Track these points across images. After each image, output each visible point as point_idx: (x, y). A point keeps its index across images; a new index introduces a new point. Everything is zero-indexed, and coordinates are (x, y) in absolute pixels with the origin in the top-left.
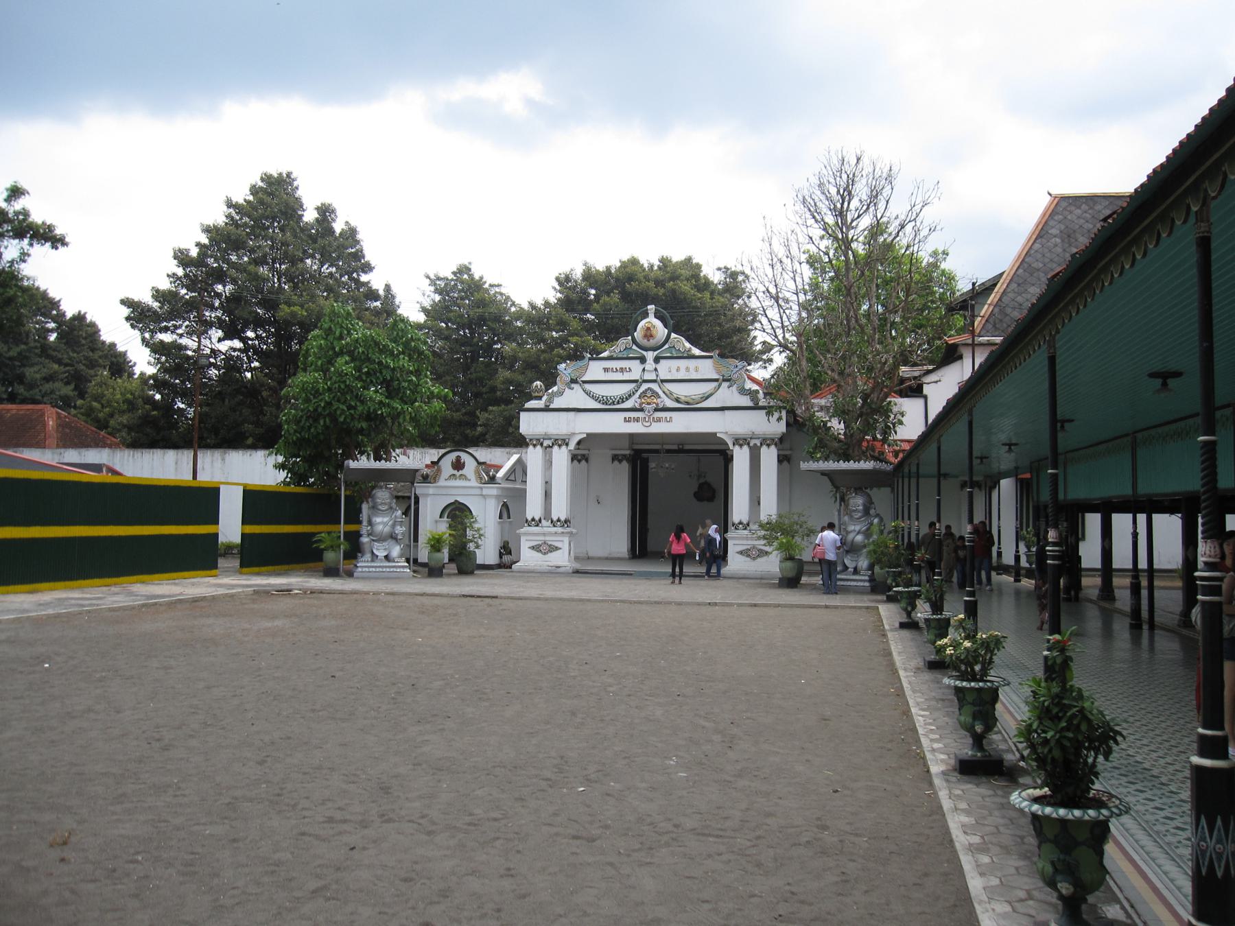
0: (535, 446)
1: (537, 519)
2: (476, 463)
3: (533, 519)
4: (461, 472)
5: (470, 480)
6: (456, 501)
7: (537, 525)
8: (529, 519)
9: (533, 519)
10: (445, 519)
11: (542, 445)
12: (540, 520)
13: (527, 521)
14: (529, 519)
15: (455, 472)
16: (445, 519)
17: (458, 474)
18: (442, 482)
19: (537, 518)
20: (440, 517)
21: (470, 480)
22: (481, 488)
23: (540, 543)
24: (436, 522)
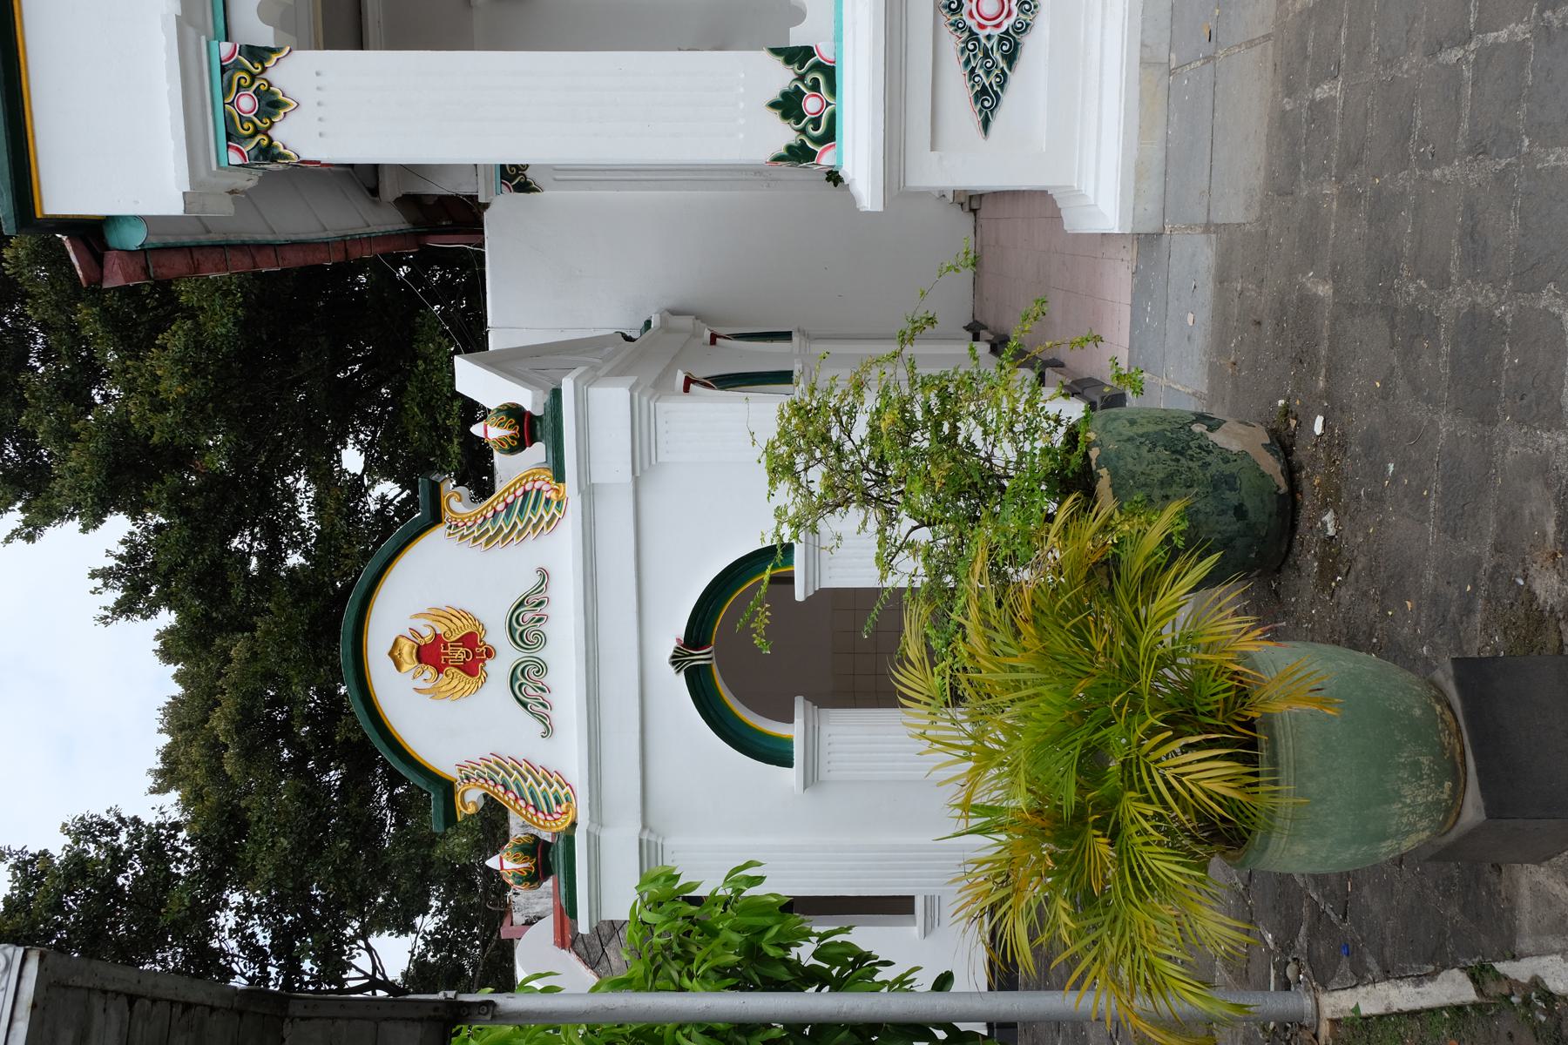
0: (271, 105)
1: (782, 77)
2: (439, 532)
3: (788, 106)
4: (496, 636)
5: (544, 574)
6: (676, 660)
7: (829, 72)
8: (784, 134)
9: (788, 106)
10: (795, 731)
11: (258, 54)
12: (797, 56)
13: (798, 154)
14: (784, 134)
15: (498, 669)
16: (795, 731)
17: (506, 657)
18: (574, 768)
19: (782, 77)
20: (785, 761)
21: (544, 574)
22: (589, 492)
23: (952, 43)
24: (811, 779)
